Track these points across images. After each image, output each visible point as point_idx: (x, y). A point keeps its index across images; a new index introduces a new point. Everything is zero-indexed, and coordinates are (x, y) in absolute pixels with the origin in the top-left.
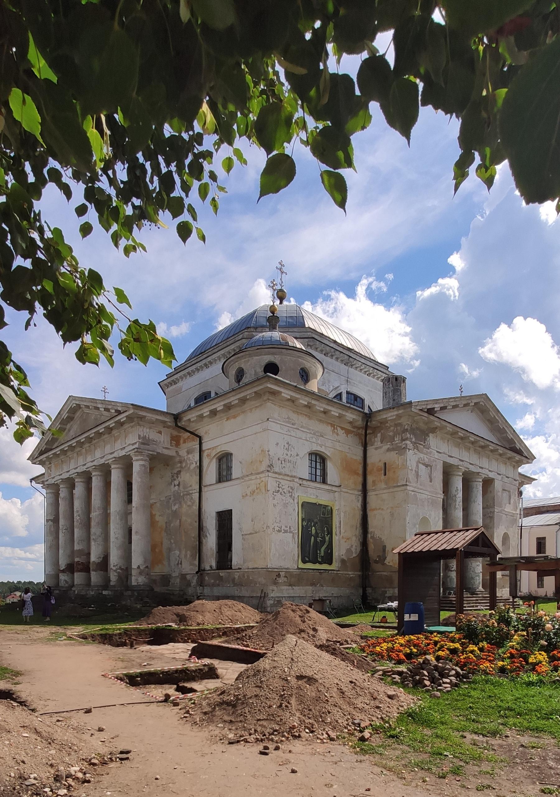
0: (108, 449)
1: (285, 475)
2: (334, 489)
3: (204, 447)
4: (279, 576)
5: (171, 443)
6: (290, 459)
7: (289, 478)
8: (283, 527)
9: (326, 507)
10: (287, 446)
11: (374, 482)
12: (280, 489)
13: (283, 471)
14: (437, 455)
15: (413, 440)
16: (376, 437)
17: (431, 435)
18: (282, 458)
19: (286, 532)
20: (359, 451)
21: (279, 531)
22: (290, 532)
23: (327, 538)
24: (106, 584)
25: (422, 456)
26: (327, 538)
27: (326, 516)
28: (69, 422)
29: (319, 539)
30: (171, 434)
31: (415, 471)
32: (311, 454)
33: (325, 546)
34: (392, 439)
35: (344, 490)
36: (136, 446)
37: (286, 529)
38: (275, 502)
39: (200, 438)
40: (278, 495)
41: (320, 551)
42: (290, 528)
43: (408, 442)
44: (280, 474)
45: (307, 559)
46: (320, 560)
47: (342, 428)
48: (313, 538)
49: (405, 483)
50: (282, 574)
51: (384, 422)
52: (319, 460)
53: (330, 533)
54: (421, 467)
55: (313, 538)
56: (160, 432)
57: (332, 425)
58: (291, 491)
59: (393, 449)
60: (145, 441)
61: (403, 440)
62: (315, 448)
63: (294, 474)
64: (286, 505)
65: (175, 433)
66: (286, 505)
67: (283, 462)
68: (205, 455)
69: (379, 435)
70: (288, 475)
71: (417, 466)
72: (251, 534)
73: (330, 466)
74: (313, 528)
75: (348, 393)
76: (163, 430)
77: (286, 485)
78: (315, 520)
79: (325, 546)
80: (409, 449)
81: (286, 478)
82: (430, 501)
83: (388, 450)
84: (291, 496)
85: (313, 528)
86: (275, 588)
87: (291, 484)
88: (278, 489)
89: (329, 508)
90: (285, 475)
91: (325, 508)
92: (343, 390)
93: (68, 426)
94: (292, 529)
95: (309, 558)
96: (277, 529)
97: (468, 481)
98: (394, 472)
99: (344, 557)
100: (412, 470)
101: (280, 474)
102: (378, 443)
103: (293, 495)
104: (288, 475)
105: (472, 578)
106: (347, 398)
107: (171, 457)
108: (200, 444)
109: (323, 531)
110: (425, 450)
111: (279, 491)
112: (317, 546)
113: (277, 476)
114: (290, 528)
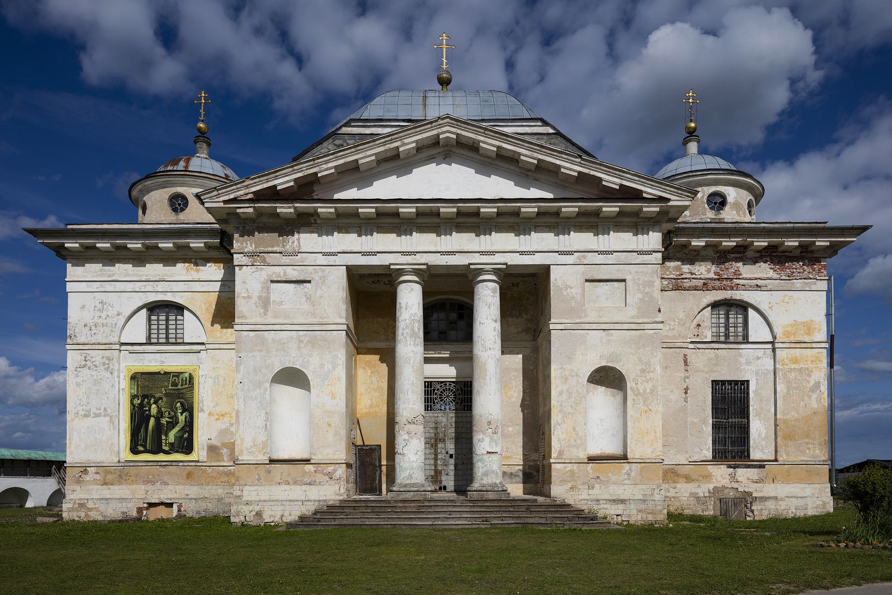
4: (85, 472)
6: (105, 321)
8: (94, 410)
9: (178, 374)
12: (88, 363)
18: (90, 322)
21: (86, 416)
23: (182, 418)
26: (182, 418)
27: (179, 387)
29: (164, 421)
33: (177, 429)
38: (79, 380)
40: (85, 371)
41: (166, 435)
42: (105, 410)
45: (141, 448)
46: (167, 448)
48: (152, 421)
50: (91, 470)
53: (189, 409)
55: (152, 421)
58: (107, 362)
64: (97, 382)
67: (93, 328)
74: (154, 406)
77: (97, 356)
78: (158, 395)
79: (177, 429)
81: (97, 347)
84: (107, 369)
85: (154, 406)
86: (78, 488)
88: (84, 363)
89: (187, 375)
91: (178, 377)
95: (145, 447)
96: (83, 413)
99: (214, 442)
103: (111, 367)
109: (173, 409)
111: (84, 366)
112: (160, 429)
114: (105, 410)
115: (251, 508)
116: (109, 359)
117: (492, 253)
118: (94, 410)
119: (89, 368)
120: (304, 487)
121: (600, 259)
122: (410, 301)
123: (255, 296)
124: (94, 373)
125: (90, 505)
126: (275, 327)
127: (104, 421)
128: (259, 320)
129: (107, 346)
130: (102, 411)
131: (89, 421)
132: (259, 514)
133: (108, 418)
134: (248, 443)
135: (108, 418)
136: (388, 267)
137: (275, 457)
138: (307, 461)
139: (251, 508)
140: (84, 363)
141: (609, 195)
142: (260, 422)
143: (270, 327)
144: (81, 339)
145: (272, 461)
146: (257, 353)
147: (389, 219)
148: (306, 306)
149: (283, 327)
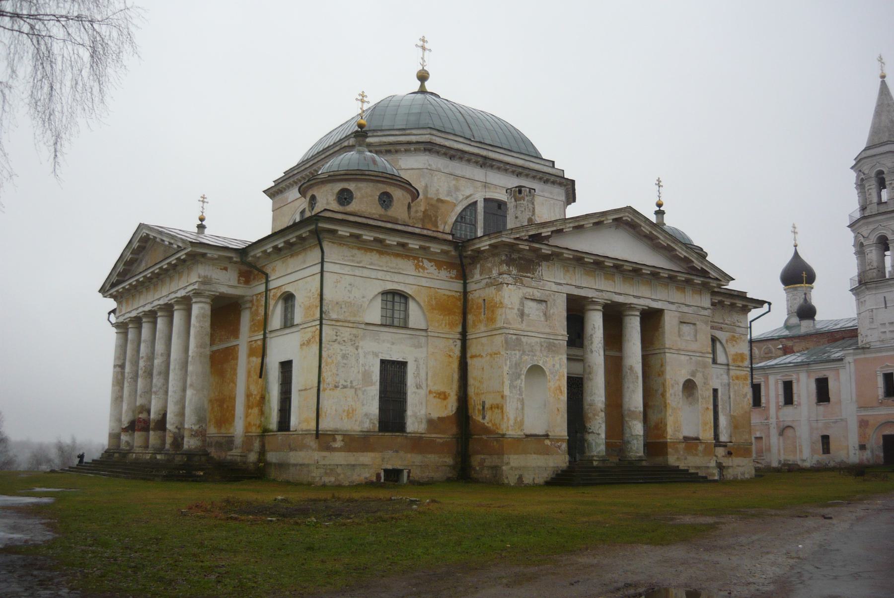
0: (174, 286)
1: (345, 321)
2: (418, 333)
3: (272, 285)
5: (239, 280)
7: (351, 325)
10: (349, 288)
11: (473, 321)
13: (341, 317)
14: (554, 288)
15: (514, 272)
16: (476, 268)
17: (544, 264)
19: (345, 387)
20: (458, 286)
21: (336, 387)
22: (352, 387)
24: (160, 449)
25: (530, 290)
28: (141, 252)
30: (240, 270)
31: (518, 310)
32: (385, 293)
34: (490, 270)
35: (432, 334)
36: (196, 287)
37: (345, 384)
39: (267, 276)
40: (336, 346)
42: (351, 382)
43: (505, 276)
44: (337, 321)
47: (430, 260)
49: (502, 325)
50: (339, 438)
51: (479, 251)
52: (395, 298)
54: (530, 305)
56: (226, 269)
57: (415, 258)
59: (492, 284)
60: (206, 281)
61: (500, 274)
62: (390, 286)
63: (357, 319)
65: (244, 268)
66: (344, 357)
68: (272, 293)
69: (478, 266)
70: (349, 322)
71: (522, 304)
72: (306, 390)
73: (412, 305)
75: (485, 200)
76: (229, 266)
77: (346, 333)
80: (508, 284)
81: (347, 324)
82: (545, 345)
83: (488, 285)
87: (354, 331)
90: (345, 321)
92: (479, 197)
93: (141, 256)
94: (354, 384)
97: (614, 316)
98: (493, 312)
100: (512, 308)
101: (337, 321)
102: (477, 277)
104: (349, 322)
105: (629, 442)
106: (485, 207)
107: (243, 297)
108: (267, 282)
110: (534, 284)
113: (334, 323)
114: (351, 382)
115: (516, 473)
116: (356, 336)
117: (639, 297)
118: (342, 382)
119: (339, 343)
120: (546, 456)
121: (685, 309)
122: (595, 322)
123: (517, 306)
124: (343, 348)
125: (339, 470)
126: (529, 334)
127: (350, 392)
128: (519, 327)
129: (355, 325)
130: (348, 383)
131: (338, 392)
132: (520, 478)
133: (353, 390)
134: (511, 422)
135: (353, 390)
136: (586, 298)
137: (528, 432)
138: (547, 436)
139: (516, 473)
140: (335, 338)
141: (693, 270)
142: (520, 406)
143: (526, 333)
144: (334, 316)
145: (527, 436)
146: (517, 352)
147: (597, 265)
148: (543, 319)
149: (533, 334)
